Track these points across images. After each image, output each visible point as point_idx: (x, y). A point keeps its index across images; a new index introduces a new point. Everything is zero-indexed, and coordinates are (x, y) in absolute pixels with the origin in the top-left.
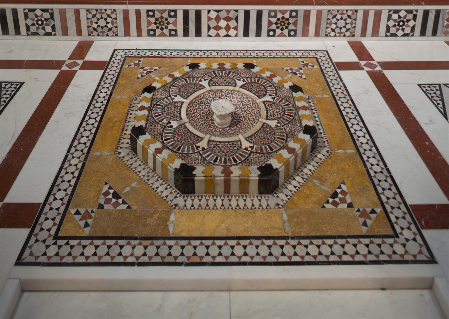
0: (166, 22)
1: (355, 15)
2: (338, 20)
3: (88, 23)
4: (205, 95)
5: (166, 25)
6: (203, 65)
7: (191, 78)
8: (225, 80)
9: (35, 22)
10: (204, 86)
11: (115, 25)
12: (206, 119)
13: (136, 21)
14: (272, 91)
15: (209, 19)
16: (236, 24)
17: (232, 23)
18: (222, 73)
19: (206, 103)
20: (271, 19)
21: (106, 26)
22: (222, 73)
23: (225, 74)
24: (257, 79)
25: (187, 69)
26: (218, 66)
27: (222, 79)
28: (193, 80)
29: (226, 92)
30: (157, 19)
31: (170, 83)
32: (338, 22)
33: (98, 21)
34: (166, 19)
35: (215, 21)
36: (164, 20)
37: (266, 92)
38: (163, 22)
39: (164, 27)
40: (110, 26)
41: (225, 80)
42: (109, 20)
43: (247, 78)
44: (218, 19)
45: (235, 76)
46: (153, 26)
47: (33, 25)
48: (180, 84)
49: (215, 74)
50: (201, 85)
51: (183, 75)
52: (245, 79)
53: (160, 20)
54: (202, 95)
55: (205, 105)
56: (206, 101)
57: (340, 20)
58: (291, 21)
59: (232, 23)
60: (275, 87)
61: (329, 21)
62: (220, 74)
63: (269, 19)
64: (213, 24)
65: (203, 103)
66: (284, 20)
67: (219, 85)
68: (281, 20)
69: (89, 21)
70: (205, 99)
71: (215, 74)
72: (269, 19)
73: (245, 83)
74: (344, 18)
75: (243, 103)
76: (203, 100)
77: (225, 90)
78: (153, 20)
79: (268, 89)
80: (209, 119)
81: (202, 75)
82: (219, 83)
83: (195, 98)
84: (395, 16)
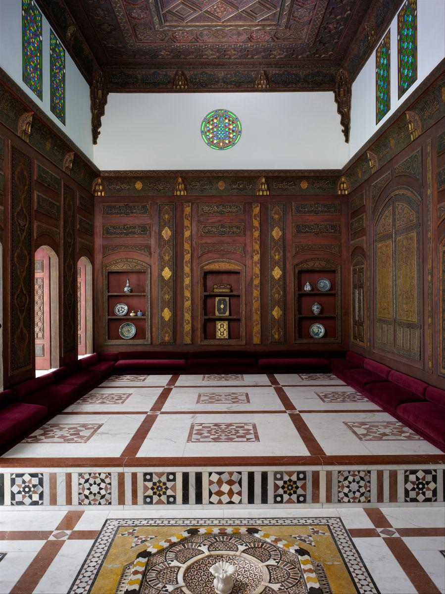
0: (164, 487)
1: (368, 477)
2: (350, 483)
3: (79, 489)
4: (204, 560)
5: (164, 490)
6: (202, 531)
7: (190, 544)
8: (226, 546)
9: (22, 490)
10: (203, 552)
11: (108, 492)
12: (205, 586)
14: (277, 555)
15: (211, 483)
17: (236, 488)
18: (223, 538)
19: (205, 569)
20: (277, 482)
21: (99, 493)
22: (223, 538)
23: (227, 539)
24: (261, 544)
25: (186, 535)
26: (219, 531)
27: (223, 544)
28: (192, 546)
29: (227, 557)
30: (155, 484)
31: (167, 548)
32: (350, 485)
33: (91, 487)
34: (165, 484)
37: (270, 557)
38: (161, 487)
39: (161, 493)
40: (103, 492)
41: (226, 546)
42: (103, 485)
43: (249, 543)
44: (220, 482)
45: (237, 541)
46: (150, 492)
47: (19, 492)
48: (178, 550)
49: (216, 539)
50: (200, 550)
51: (181, 540)
52: (248, 544)
53: (158, 484)
54: (201, 561)
55: (204, 571)
56: (206, 567)
58: (299, 484)
59: (236, 488)
60: (280, 551)
61: (340, 484)
62: (221, 539)
63: (275, 483)
64: (214, 488)
65: (201, 570)
66: (292, 483)
67: (219, 550)
68: (288, 483)
69: (81, 486)
70: (204, 565)
71: (216, 539)
72: (275, 483)
73: (247, 547)
74: (356, 480)
75: (245, 569)
76: (202, 566)
77: (226, 555)
78: (150, 485)
79: (272, 553)
80: (208, 586)
81: (202, 541)
82: (219, 548)
83: (193, 564)
84: (412, 478)
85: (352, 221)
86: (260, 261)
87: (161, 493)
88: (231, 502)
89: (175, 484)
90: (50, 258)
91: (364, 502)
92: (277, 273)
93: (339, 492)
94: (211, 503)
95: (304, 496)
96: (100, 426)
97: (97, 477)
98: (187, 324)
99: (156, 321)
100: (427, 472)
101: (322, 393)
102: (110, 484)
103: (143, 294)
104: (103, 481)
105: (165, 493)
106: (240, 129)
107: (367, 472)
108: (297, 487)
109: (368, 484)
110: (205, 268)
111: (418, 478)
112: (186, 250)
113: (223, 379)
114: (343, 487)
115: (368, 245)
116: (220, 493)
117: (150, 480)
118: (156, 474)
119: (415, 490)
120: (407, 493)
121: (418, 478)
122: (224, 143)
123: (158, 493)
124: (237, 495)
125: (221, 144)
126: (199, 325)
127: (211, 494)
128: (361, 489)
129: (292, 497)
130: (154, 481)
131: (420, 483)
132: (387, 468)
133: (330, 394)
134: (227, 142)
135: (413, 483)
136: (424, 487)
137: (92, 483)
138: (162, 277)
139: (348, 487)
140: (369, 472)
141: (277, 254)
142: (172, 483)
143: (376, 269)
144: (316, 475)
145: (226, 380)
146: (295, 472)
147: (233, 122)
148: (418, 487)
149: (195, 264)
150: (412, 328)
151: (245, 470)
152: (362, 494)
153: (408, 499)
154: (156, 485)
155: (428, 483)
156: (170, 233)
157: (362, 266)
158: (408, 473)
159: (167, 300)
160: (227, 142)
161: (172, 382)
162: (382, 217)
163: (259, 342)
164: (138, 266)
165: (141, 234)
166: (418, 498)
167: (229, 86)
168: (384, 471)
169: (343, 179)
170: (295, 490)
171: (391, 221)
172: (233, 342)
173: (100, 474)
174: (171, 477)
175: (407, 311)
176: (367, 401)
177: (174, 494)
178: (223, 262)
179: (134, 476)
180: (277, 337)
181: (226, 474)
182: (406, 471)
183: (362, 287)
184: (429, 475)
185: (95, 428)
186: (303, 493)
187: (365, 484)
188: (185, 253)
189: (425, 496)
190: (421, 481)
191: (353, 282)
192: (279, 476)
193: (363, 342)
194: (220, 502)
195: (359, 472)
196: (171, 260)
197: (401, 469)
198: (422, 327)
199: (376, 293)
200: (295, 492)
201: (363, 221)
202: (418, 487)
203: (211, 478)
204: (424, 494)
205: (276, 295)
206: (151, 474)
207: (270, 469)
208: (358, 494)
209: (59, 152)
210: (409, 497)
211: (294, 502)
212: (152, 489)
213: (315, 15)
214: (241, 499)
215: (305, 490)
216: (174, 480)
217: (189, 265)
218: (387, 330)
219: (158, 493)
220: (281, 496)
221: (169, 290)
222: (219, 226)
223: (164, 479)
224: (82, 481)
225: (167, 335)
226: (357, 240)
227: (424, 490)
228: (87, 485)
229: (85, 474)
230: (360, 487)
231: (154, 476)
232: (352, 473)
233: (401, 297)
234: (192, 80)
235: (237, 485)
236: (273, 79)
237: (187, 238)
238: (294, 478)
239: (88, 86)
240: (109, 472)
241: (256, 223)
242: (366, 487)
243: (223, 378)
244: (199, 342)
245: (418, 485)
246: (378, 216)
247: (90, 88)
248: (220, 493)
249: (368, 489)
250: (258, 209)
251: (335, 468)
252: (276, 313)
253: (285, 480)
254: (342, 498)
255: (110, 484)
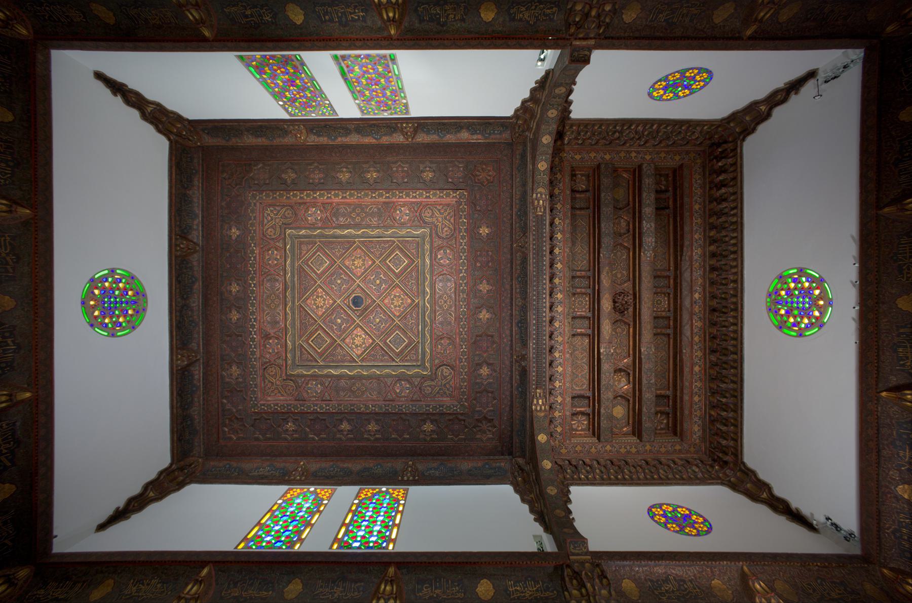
106: (119, 334)
122: (94, 308)
125: (92, 303)
134: (96, 313)
147: (128, 322)
160: (96, 313)
167: (178, 314)
209: (246, 17)
213: (313, 404)
234: (185, 262)
236: (186, 373)
239: (190, 118)
247: (188, 120)
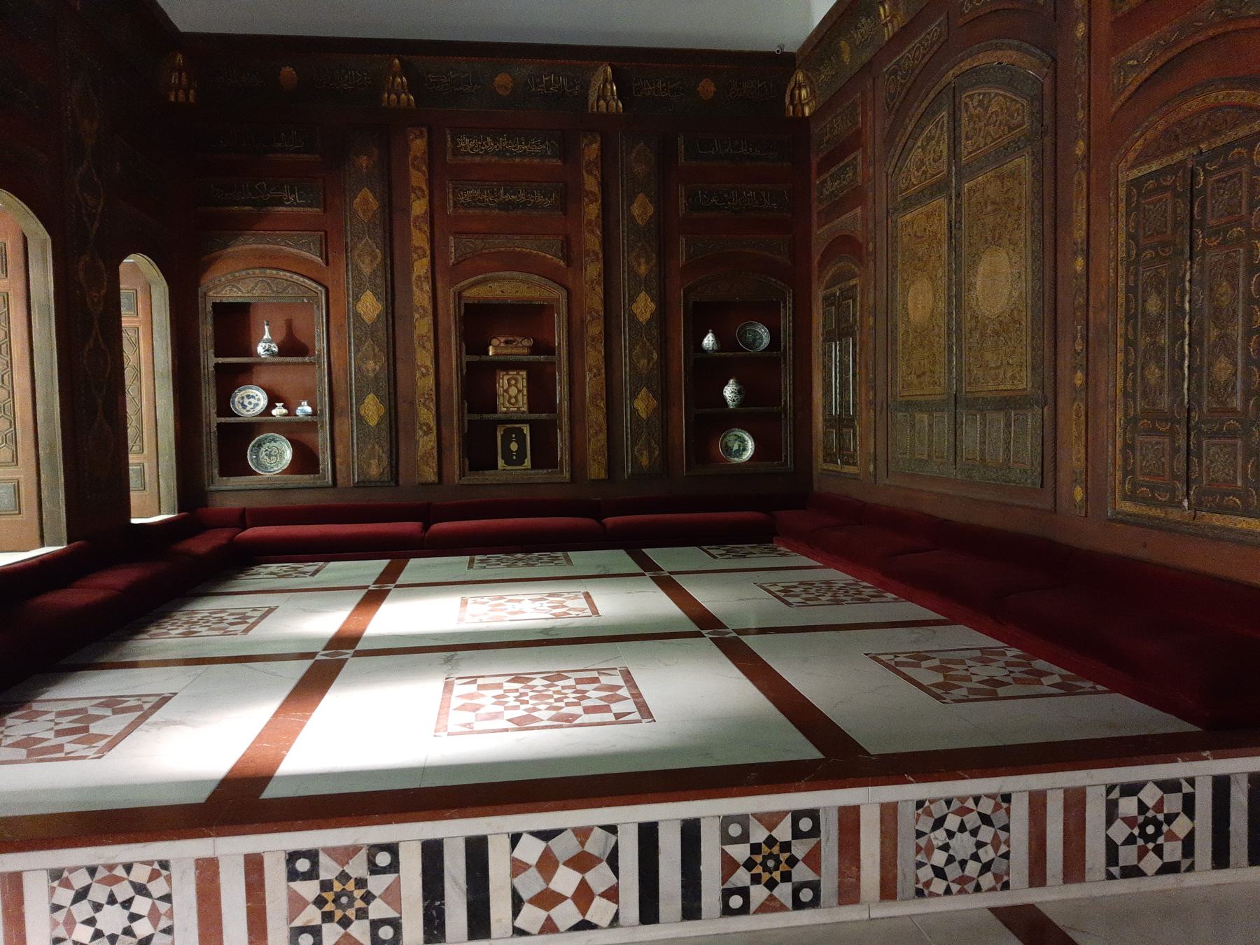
0: (358, 894)
1: (1003, 812)
2: (950, 834)
5: (359, 904)
11: (164, 924)
13: (248, 901)
15: (518, 867)
16: (612, 879)
17: (599, 878)
20: (731, 849)
30: (327, 886)
32: (952, 843)
33: (98, 916)
34: (361, 883)
35: (538, 875)
36: (350, 886)
39: (351, 913)
42: (141, 905)
44: (547, 864)
53: (338, 887)
57: (958, 835)
58: (800, 849)
59: (599, 878)
61: (922, 842)
63: (723, 851)
64: (530, 884)
66: (776, 850)
68: (765, 849)
72: (723, 851)
74: (969, 827)
78: (309, 889)
84: (1128, 806)
85: (822, 178)
86: (602, 278)
87: (351, 913)
88: (584, 926)
89: (398, 880)
90: (25, 239)
91: (993, 889)
92: (644, 307)
93: (920, 865)
94: (519, 932)
95: (815, 886)
96: (164, 700)
97: (118, 880)
98: (426, 433)
99: (346, 428)
100: (1169, 786)
101: (775, 584)
102: (167, 898)
103: (307, 359)
104: (141, 890)
105: (362, 913)
107: (999, 799)
108: (792, 861)
109: (1003, 835)
110: (467, 294)
111: (1142, 807)
112: (417, 248)
113: (520, 564)
114: (929, 850)
115: (871, 226)
116: (548, 899)
117: (312, 874)
118: (331, 852)
119: (1134, 842)
120: (1112, 849)
121: (1142, 807)
123: (338, 915)
124: (604, 902)
126: (456, 437)
127: (517, 903)
128: (981, 852)
129: (776, 892)
130: (324, 875)
131: (1148, 821)
132: (1054, 783)
133: (796, 587)
135: (1130, 821)
136: (1158, 832)
137: (102, 899)
138: (358, 316)
139: (945, 848)
140: (1007, 798)
141: (642, 260)
142: (389, 879)
143: (895, 281)
144: (849, 819)
145: (528, 564)
146: (785, 813)
148: (1143, 834)
149: (439, 285)
150: (1015, 409)
151: (628, 816)
152: (986, 868)
153: (1115, 870)
154: (331, 889)
155: (1170, 818)
156: (374, 204)
157: (852, 282)
158: (1115, 794)
159: (371, 374)
161: (389, 576)
162: (915, 144)
163: (603, 475)
164: (293, 289)
165: (299, 205)
166: (1143, 865)
168: (1049, 794)
169: (800, 77)
170: (787, 868)
171: (944, 147)
172: (542, 475)
173: (128, 868)
174: (383, 859)
175: (998, 367)
176: (896, 600)
177: (392, 914)
178: (512, 279)
179: (254, 865)
180: (645, 461)
181: (569, 835)
182: (1110, 789)
183: (853, 334)
184: (1173, 795)
185: (146, 707)
186: (809, 875)
187: (996, 836)
188: (415, 256)
189: (1161, 857)
190: (1150, 814)
191: (824, 326)
192: (735, 830)
193: (854, 464)
194: (549, 927)
195: (977, 800)
196: (379, 273)
197: (1094, 780)
198: (1050, 400)
199: (895, 340)
200: (786, 877)
201: (855, 168)
202: (1143, 834)
203: (517, 853)
204: (1159, 851)
205: (644, 362)
206: (312, 855)
207: (708, 810)
208: (973, 868)
210: (1117, 865)
211: (782, 908)
212: (320, 902)
214: (618, 910)
215: (816, 867)
216: (394, 867)
217: (427, 287)
218: (931, 425)
219: (338, 915)
220: (744, 892)
221: (377, 350)
222: (499, 190)
223: (357, 867)
224: (65, 896)
225: (374, 462)
226: (836, 222)
227: (1161, 840)
228: (83, 910)
229: (73, 870)
230: (980, 845)
231: (324, 859)
232: (956, 805)
233: (977, 335)
235: (604, 868)
237: (417, 217)
238: (783, 832)
240: (163, 857)
241: (591, 183)
242: (996, 843)
243: (520, 560)
244: (456, 478)
245: (1143, 827)
246: (901, 145)
248: (548, 899)
249: (1003, 849)
250: (595, 146)
251: (906, 793)
252: (643, 404)
253: (753, 840)
254: (928, 884)
255: (167, 898)
